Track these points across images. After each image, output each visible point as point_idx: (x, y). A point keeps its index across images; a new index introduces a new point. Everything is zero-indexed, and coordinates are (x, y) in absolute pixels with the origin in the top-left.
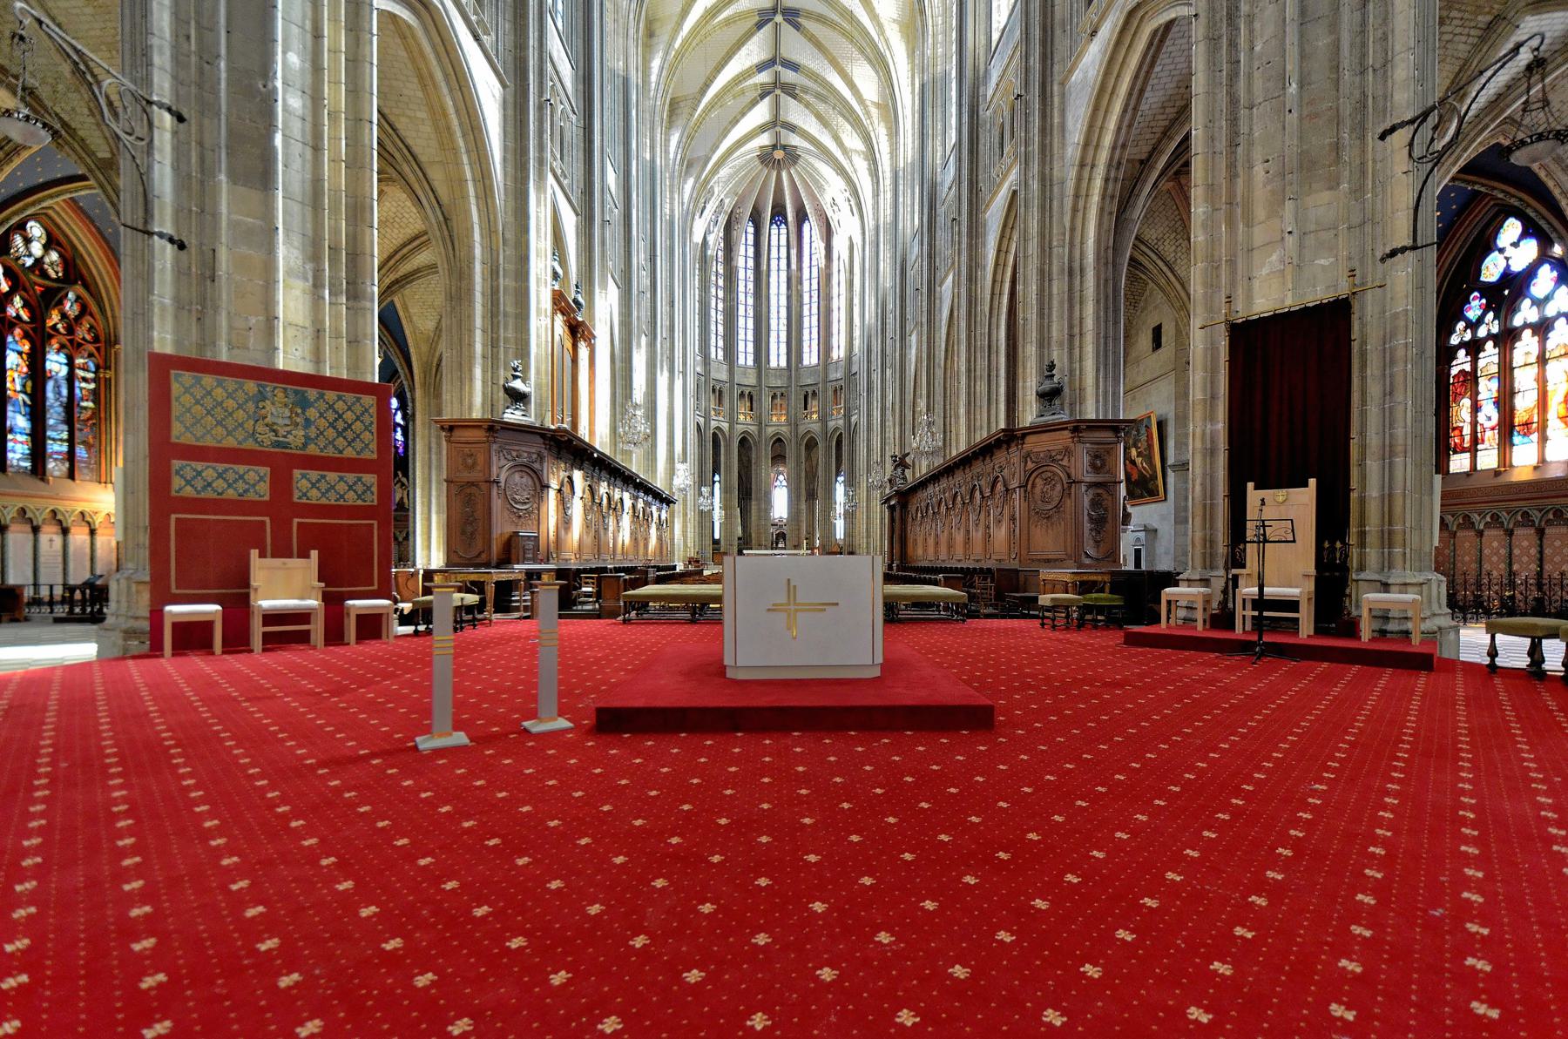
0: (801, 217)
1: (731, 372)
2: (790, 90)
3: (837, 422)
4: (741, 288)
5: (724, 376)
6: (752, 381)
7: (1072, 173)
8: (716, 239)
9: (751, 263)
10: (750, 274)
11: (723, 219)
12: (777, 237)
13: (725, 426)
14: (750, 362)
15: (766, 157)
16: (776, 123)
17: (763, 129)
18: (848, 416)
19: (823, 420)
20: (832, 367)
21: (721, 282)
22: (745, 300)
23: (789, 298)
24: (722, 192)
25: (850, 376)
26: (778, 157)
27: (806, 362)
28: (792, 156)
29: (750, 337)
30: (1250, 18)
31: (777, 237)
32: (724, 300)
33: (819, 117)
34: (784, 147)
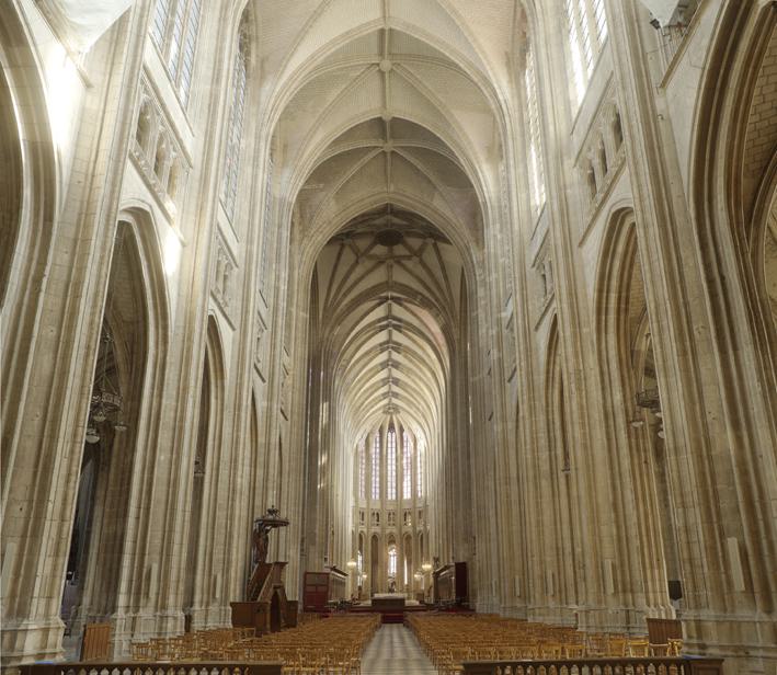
0: (402, 430)
1: (368, 503)
3: (420, 528)
5: (365, 506)
6: (377, 507)
9: (378, 450)
10: (378, 456)
13: (365, 530)
14: (378, 496)
17: (385, 406)
18: (425, 526)
19: (414, 526)
20: (417, 501)
22: (376, 469)
24: (367, 427)
25: (426, 506)
26: (391, 410)
27: (405, 497)
28: (396, 409)
29: (378, 485)
31: (391, 438)
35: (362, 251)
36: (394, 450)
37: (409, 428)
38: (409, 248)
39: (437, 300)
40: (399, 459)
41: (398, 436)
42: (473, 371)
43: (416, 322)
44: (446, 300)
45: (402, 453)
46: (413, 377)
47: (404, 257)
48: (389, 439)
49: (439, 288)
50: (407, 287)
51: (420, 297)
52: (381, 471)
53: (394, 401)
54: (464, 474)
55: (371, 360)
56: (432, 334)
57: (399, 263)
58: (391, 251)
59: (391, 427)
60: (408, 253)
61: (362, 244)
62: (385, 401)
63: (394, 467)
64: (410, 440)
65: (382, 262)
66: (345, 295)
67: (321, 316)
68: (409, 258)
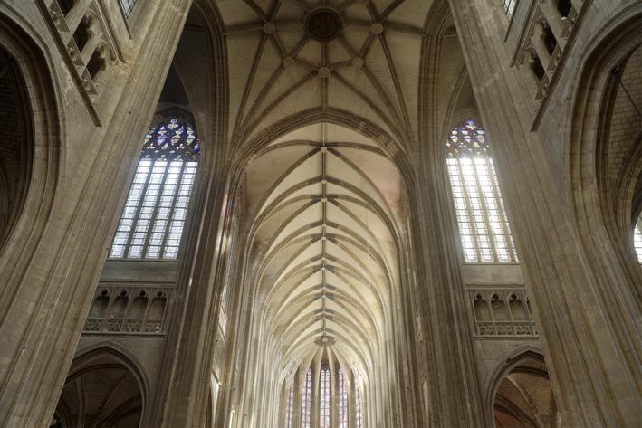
0: (337, 366)
2: (330, 318)
4: (304, 405)
7: (428, 421)
8: (291, 380)
9: (309, 391)
10: (309, 397)
11: (295, 371)
12: (325, 377)
15: (319, 342)
16: (323, 329)
17: (317, 331)
21: (292, 403)
23: (331, 411)
26: (325, 340)
30: (442, 420)
31: (325, 377)
32: (293, 413)
33: (345, 329)
34: (328, 337)
35: (288, 51)
36: (328, 390)
37: (347, 366)
38: (350, 49)
39: (386, 120)
40: (334, 403)
41: (332, 373)
42: (476, 80)
43: (356, 180)
44: (397, 117)
45: (337, 394)
46: (352, 280)
47: (340, 64)
48: (323, 377)
49: (389, 104)
50: (346, 113)
51: (362, 124)
52: (312, 416)
53: (330, 324)
54: (445, 346)
55: (301, 250)
56: (378, 191)
57: (334, 73)
58: (325, 53)
59: (325, 365)
60: (348, 57)
61: (289, 38)
62: (318, 325)
63: (328, 412)
64: (346, 377)
65: (315, 73)
66: (265, 114)
67: (230, 135)
68: (349, 63)
